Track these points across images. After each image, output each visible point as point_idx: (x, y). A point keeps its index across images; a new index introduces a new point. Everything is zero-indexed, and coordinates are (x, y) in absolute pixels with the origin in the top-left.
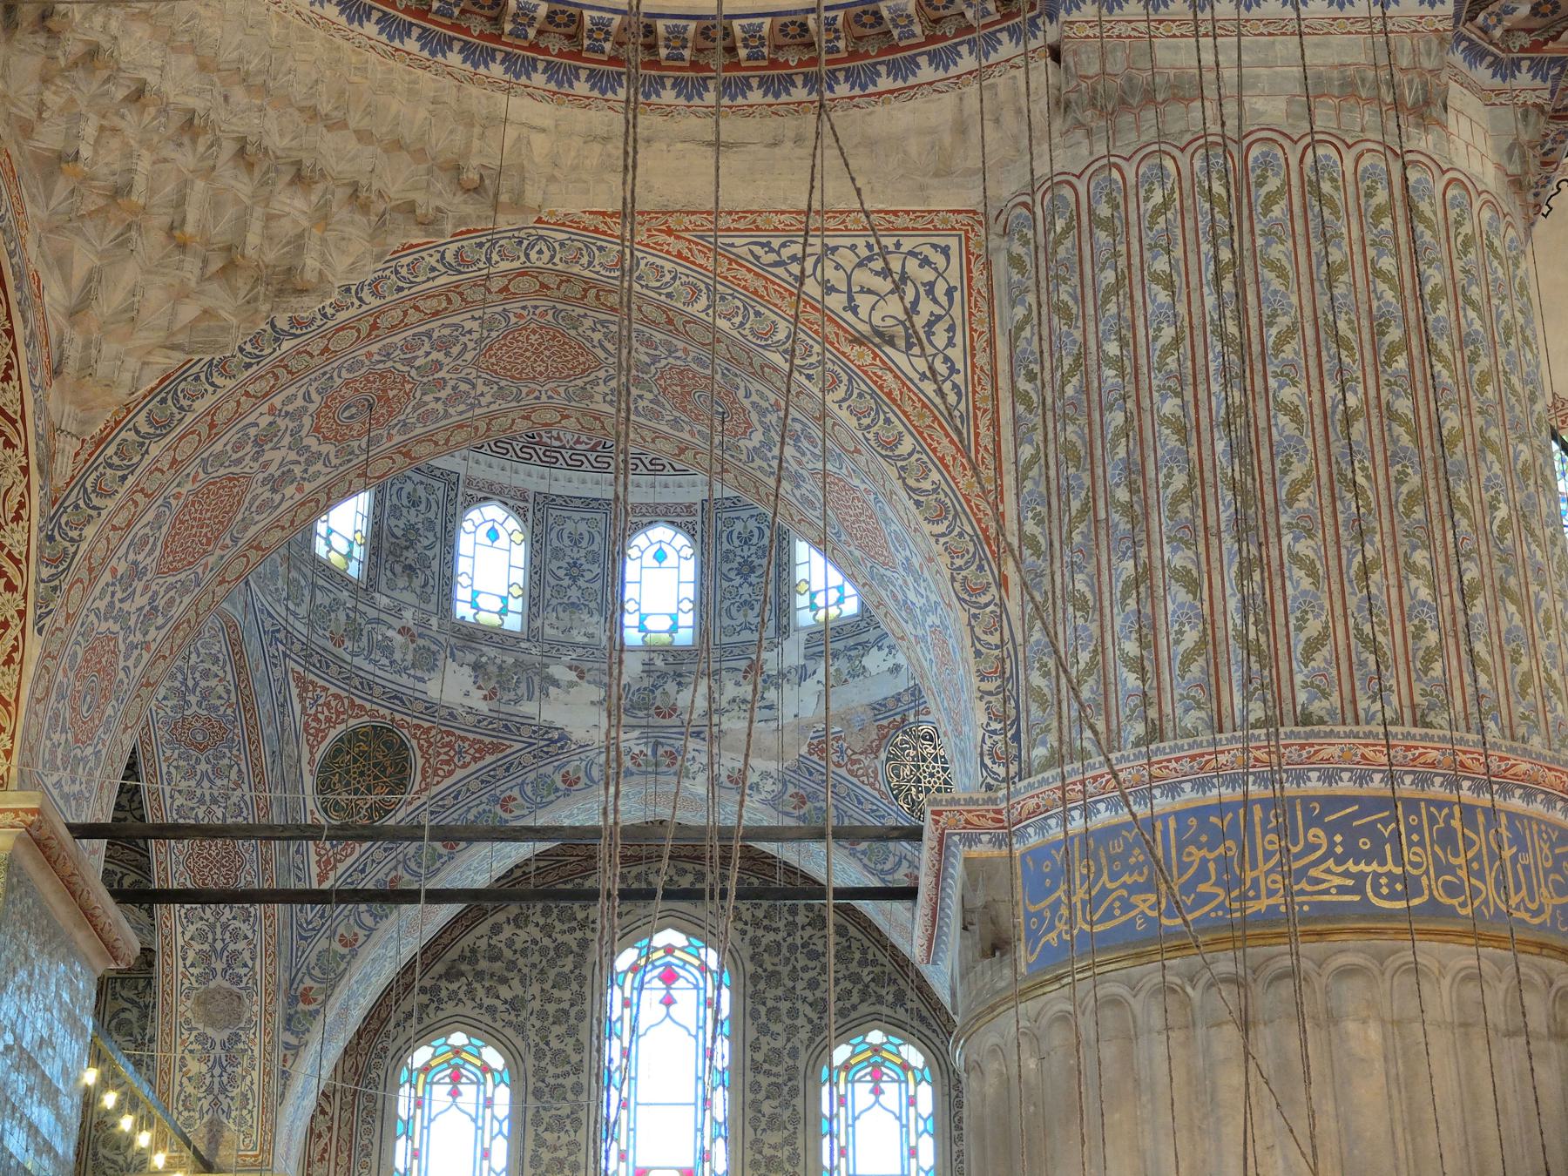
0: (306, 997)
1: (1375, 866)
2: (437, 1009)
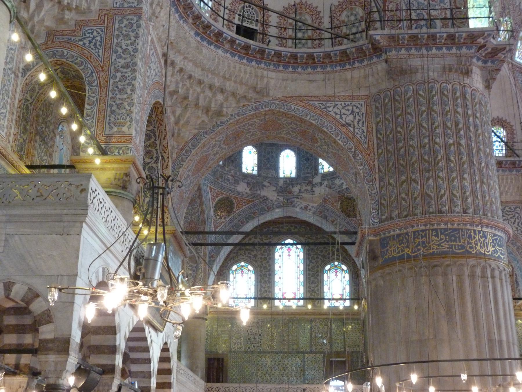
0: (212, 257)
1: (455, 243)
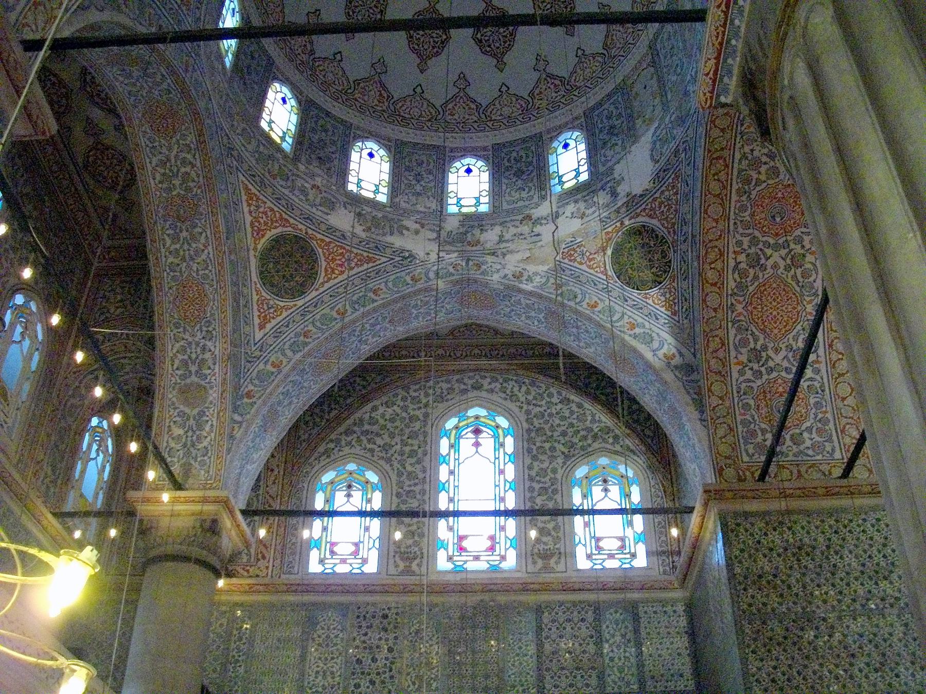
2: (339, 450)
